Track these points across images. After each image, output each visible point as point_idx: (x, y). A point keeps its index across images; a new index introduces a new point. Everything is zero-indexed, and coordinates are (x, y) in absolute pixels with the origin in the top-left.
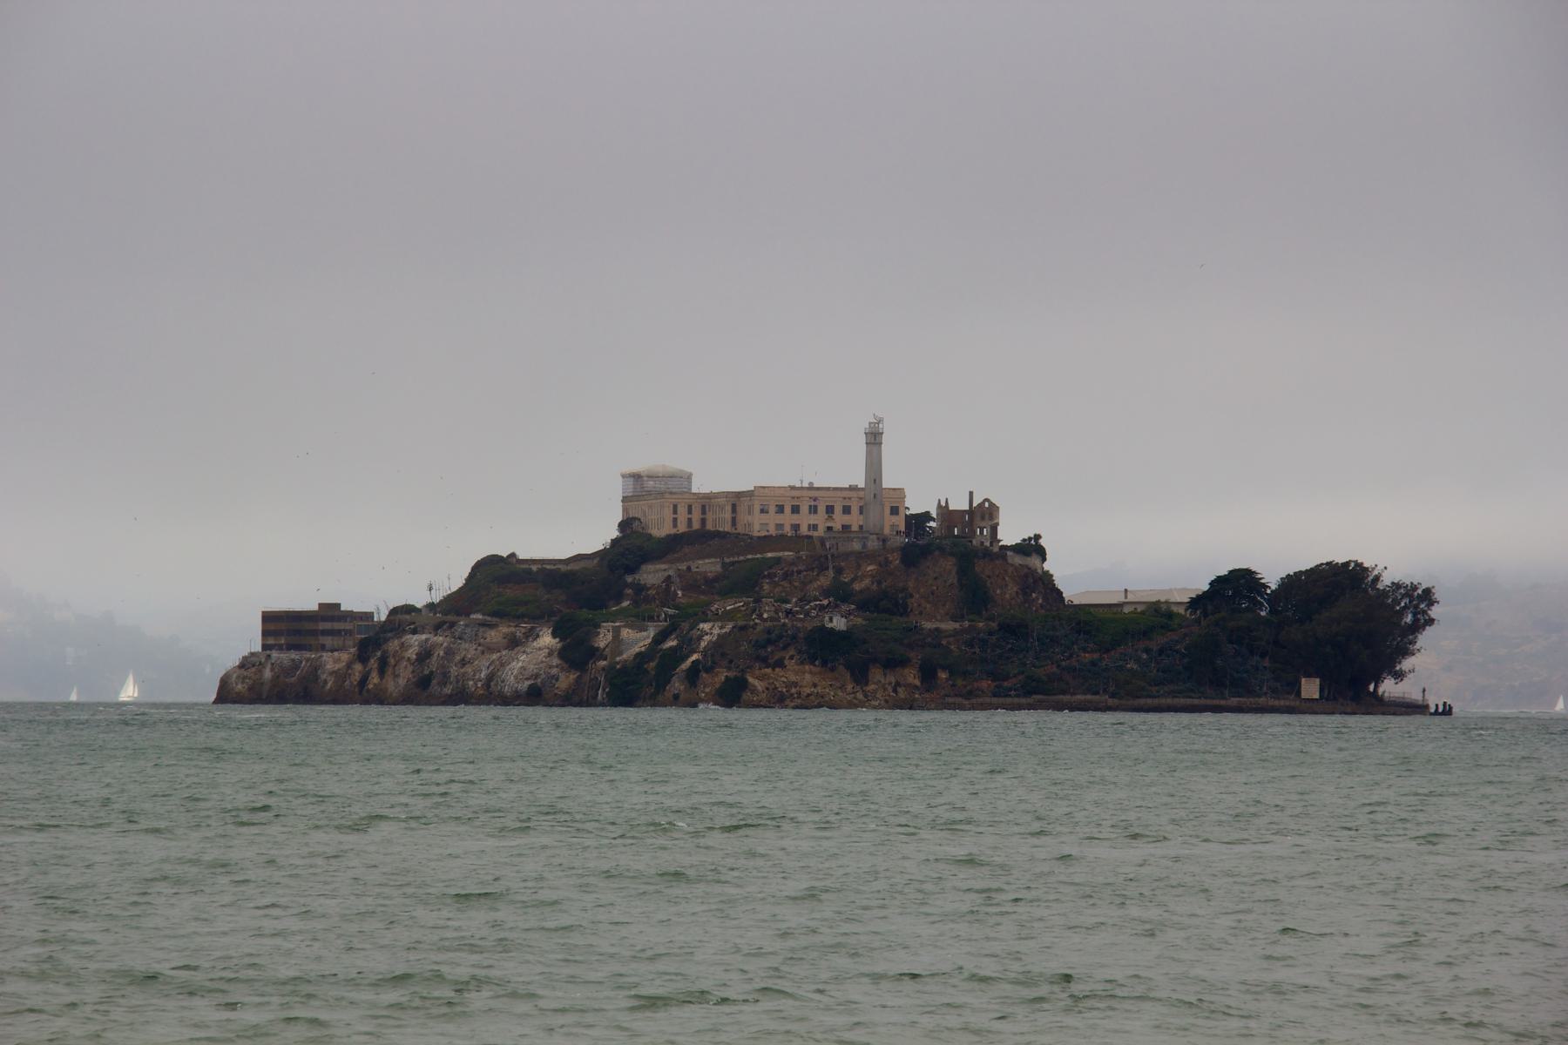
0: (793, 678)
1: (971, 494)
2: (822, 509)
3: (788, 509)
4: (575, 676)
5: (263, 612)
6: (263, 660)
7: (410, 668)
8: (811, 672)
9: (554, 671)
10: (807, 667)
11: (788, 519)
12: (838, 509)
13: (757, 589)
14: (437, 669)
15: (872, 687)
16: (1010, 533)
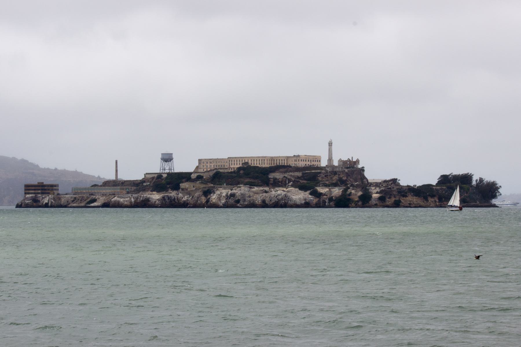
0: (411, 200)
1: (352, 157)
2: (310, 161)
3: (305, 161)
4: (317, 200)
5: (25, 185)
6: (130, 196)
7: (224, 199)
8: (415, 198)
9: (312, 198)
10: (414, 197)
11: (308, 163)
12: (312, 161)
13: (317, 179)
14: (241, 198)
15: (429, 202)
16: (360, 166)
